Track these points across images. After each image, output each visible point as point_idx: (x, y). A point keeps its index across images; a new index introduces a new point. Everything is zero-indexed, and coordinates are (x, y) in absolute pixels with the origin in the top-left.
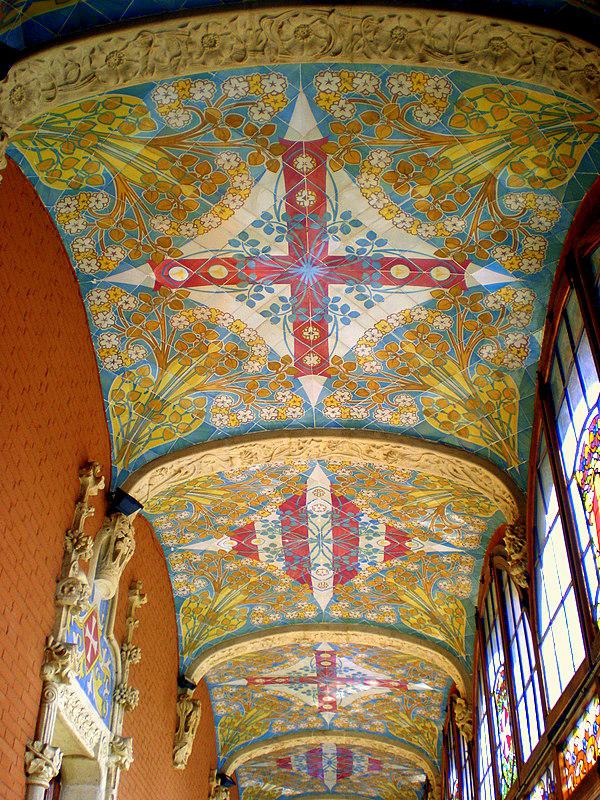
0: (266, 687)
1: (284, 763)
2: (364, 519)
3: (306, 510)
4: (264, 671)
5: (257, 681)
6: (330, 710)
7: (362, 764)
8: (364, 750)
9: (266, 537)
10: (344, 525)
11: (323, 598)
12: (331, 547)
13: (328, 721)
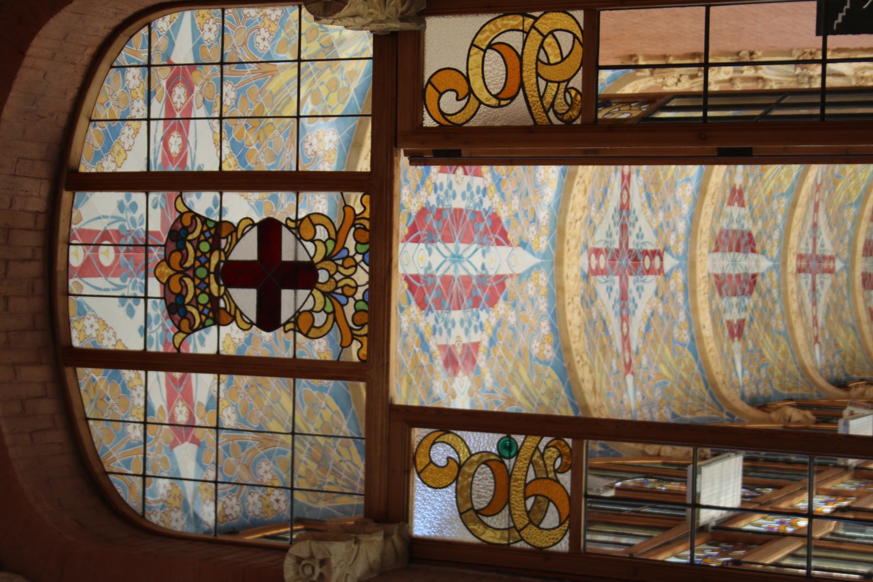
0: (634, 348)
1: (737, 330)
2: (433, 201)
3: (424, 277)
4: (614, 349)
5: (627, 360)
6: (662, 260)
7: (735, 216)
8: (718, 215)
9: (453, 332)
10: (440, 228)
11: (523, 261)
12: (463, 246)
13: (677, 262)
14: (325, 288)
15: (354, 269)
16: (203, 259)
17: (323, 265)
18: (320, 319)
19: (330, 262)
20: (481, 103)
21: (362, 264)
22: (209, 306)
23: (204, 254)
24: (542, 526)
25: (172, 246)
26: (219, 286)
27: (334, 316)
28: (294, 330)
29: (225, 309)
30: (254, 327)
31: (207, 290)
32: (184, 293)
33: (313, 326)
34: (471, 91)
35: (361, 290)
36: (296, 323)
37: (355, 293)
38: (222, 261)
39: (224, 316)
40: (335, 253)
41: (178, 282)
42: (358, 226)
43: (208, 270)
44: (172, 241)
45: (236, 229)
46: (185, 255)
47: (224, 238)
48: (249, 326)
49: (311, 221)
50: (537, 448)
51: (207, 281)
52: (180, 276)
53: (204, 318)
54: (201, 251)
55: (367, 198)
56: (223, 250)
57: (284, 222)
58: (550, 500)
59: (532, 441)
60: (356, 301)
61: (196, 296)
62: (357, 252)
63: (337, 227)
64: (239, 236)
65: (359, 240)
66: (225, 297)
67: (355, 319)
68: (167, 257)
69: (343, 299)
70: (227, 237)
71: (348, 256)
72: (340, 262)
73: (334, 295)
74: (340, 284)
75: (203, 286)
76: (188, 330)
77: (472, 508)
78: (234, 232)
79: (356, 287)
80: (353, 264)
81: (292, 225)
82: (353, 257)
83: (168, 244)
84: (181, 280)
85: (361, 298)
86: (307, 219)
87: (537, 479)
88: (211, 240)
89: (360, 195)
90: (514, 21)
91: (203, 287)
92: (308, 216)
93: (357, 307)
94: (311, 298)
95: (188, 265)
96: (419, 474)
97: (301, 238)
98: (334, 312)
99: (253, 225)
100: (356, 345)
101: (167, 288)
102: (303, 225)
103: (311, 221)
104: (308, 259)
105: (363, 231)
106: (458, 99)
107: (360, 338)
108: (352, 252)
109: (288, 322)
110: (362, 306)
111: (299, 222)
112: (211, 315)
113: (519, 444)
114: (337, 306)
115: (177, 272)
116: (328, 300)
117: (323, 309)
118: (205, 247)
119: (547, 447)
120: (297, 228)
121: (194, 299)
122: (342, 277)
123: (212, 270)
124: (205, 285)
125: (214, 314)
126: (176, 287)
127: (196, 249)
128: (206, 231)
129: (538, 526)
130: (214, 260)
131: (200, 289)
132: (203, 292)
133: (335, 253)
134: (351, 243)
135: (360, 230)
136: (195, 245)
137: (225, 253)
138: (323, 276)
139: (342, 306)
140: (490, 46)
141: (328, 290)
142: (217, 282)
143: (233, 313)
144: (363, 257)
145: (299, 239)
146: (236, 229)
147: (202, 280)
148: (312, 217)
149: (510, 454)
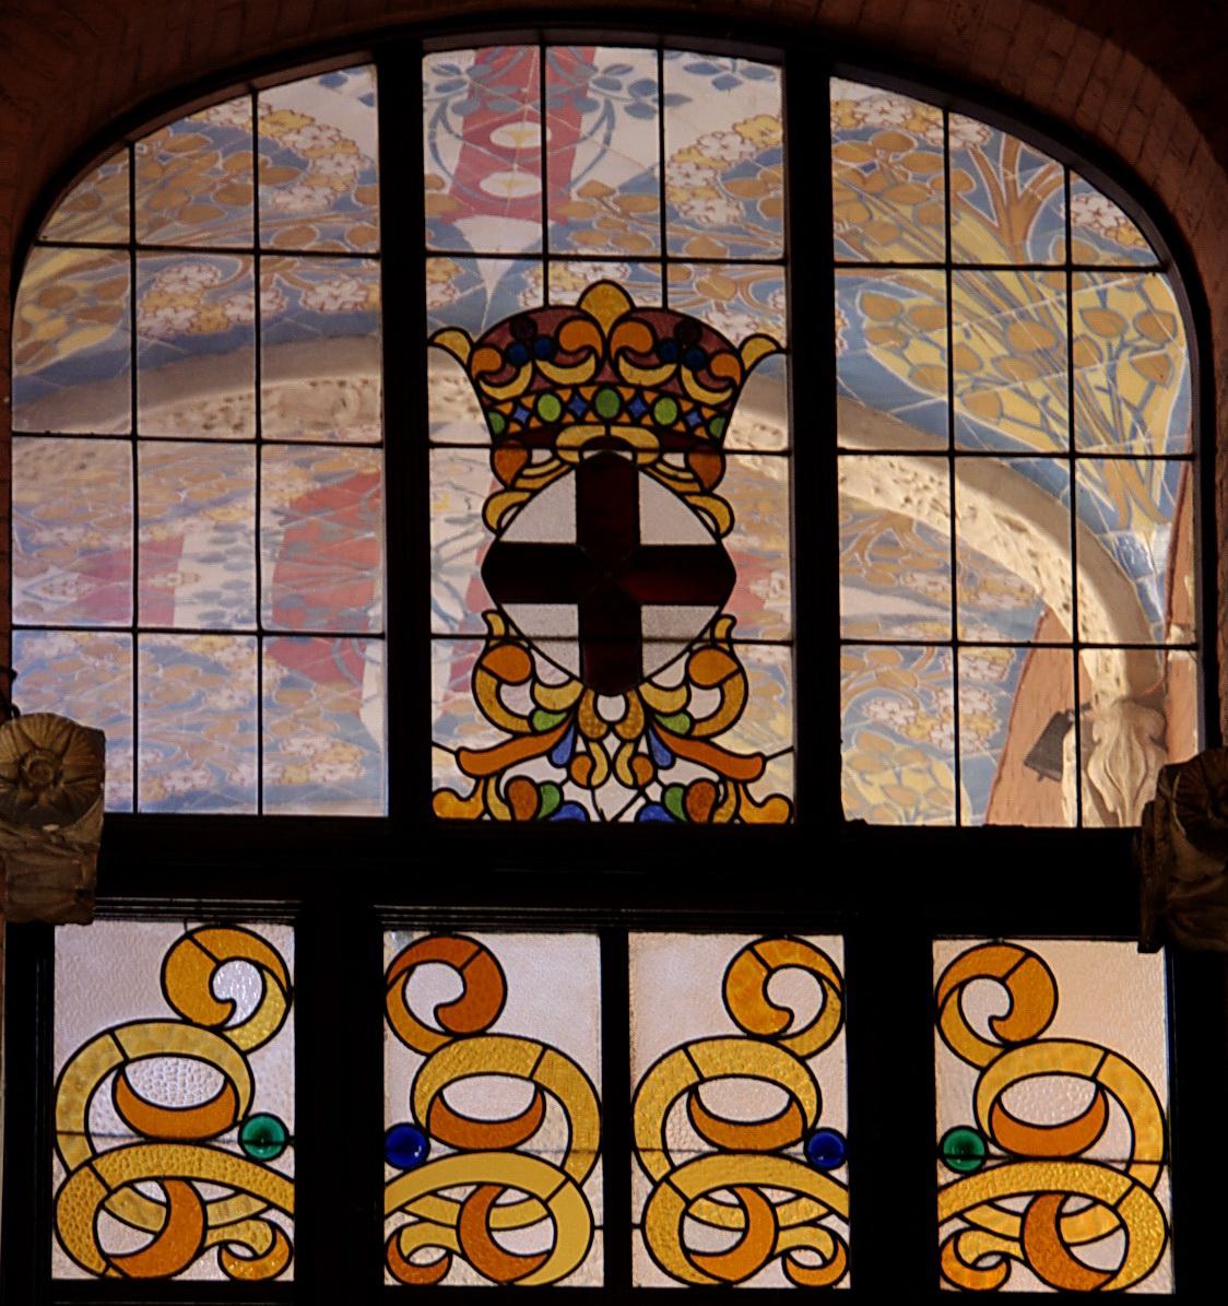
14: (585, 711)
15: (630, 781)
16: (636, 409)
17: (636, 708)
18: (518, 700)
19: (642, 724)
20: (983, 1071)
21: (641, 802)
22: (534, 423)
23: (650, 410)
24: (103, 1215)
25: (666, 330)
26: (580, 449)
27: (523, 733)
28: (489, 637)
29: (529, 464)
30: (493, 537)
31: (569, 418)
32: (560, 357)
33: (501, 681)
34: (1008, 1046)
35: (583, 797)
36: (506, 640)
37: (577, 783)
38: (635, 457)
39: (512, 458)
40: (662, 734)
41: (588, 343)
42: (721, 788)
43: (614, 421)
44: (677, 329)
45: (707, 492)
46: (645, 362)
47: (686, 460)
48: (493, 521)
49: (730, 676)
50: (271, 1206)
51: (590, 417)
52: (599, 348)
53: (507, 409)
54: (656, 401)
55: (779, 814)
56: (660, 460)
57: (725, 611)
58: (157, 1236)
59: (286, 1195)
60: (559, 787)
61: (554, 388)
62: (665, 788)
63: (718, 740)
64: (693, 500)
65: (692, 791)
66: (556, 463)
67: (520, 783)
68: (640, 315)
69: (562, 754)
70: (688, 468)
71: (656, 767)
72: (643, 748)
73: (571, 735)
74: (594, 747)
75: (578, 406)
76: (476, 368)
77: (127, 1061)
78: (700, 488)
79: (592, 788)
80: (641, 781)
81: (720, 632)
82: (655, 778)
83: (669, 318)
84: (591, 350)
85: (567, 798)
86: (735, 667)
87: (204, 1204)
88: (681, 427)
89: (789, 792)
90: (1153, 1142)
91: (578, 408)
92: (741, 670)
93: (547, 787)
94: (563, 677)
95: (624, 366)
96: (189, 935)
97: (693, 654)
98: (535, 733)
99: (718, 535)
100: (466, 786)
101: (569, 313)
102: (720, 655)
103: (730, 676)
104: (648, 670)
105: (710, 802)
106: (992, 1019)
107: (479, 794)
108: (665, 776)
109: (508, 621)
110: (551, 799)
111: (726, 647)
112: (515, 428)
113: (274, 1165)
114: (547, 742)
115: (606, 342)
116: (560, 718)
117: (539, 707)
118: (666, 412)
119: (274, 1227)
120: (713, 644)
121: (548, 385)
122: (612, 752)
123: (616, 431)
124: (579, 413)
125: (515, 435)
126: (573, 336)
127: (660, 390)
128: (700, 415)
129: (101, 1206)
130: (640, 437)
131: (572, 399)
132: (565, 408)
133: (662, 734)
134: (684, 772)
135: (713, 795)
136: (670, 387)
137: (652, 465)
138: (611, 708)
139: (548, 754)
140: (1101, 1089)
141: (581, 720)
142: (590, 444)
143: (521, 483)
144: (656, 803)
145: (688, 649)
146: (707, 492)
147: (591, 406)
148: (738, 678)
149: (248, 1142)
